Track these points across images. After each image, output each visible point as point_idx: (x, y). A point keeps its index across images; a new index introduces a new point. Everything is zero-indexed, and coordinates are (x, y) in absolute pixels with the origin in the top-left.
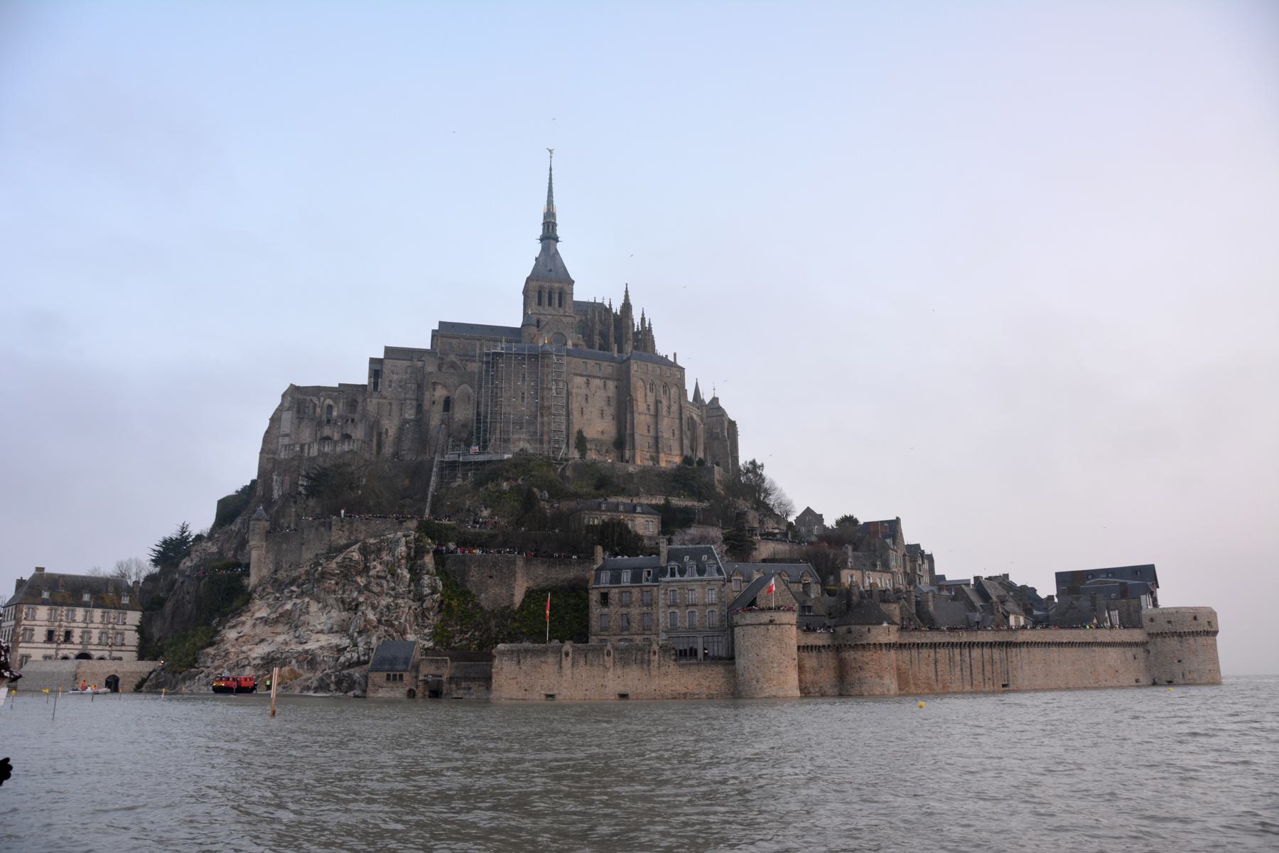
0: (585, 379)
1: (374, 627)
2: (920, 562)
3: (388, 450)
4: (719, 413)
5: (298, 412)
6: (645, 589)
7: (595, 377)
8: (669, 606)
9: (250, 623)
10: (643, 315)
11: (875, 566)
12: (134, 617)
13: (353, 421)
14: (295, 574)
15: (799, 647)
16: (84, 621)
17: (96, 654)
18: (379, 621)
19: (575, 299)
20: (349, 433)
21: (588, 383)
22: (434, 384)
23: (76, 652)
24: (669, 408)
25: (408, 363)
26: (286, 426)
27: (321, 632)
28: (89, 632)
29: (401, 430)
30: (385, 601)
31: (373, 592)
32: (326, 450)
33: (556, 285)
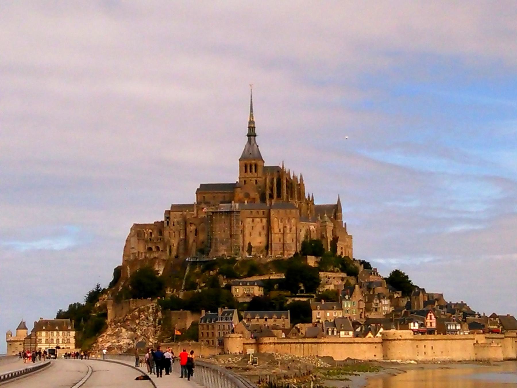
0: (251, 219)
1: (139, 337)
2: (378, 302)
5: (138, 236)
8: (218, 330)
9: (105, 336)
10: (294, 174)
11: (333, 308)
12: (73, 333)
14: (120, 318)
15: (244, 344)
16: (57, 336)
17: (61, 347)
18: (141, 335)
20: (158, 246)
21: (253, 221)
22: (191, 223)
23: (55, 346)
24: (291, 229)
25: (181, 213)
27: (125, 339)
28: (59, 339)
29: (179, 244)
30: (145, 328)
31: (140, 325)
33: (253, 162)
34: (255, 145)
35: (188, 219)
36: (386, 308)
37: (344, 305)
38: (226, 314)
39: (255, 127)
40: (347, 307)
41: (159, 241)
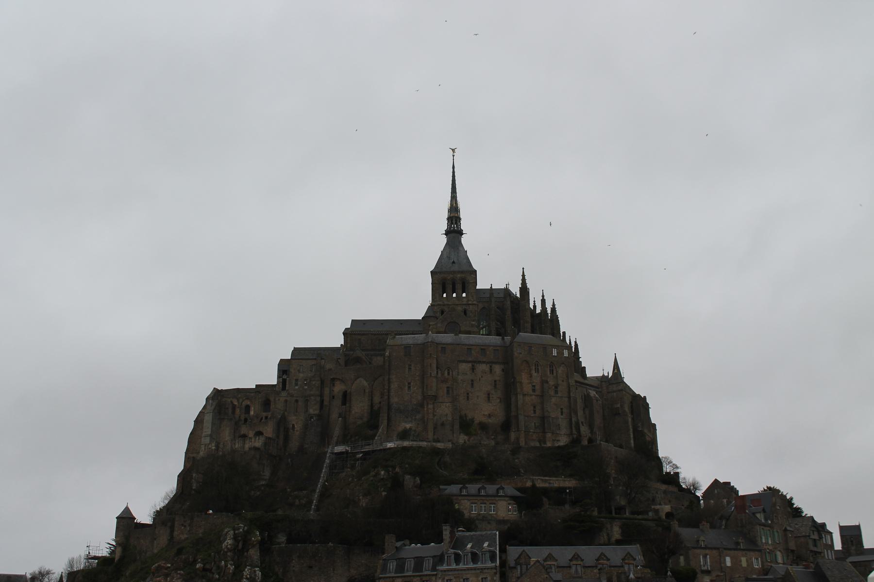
0: (470, 365)
2: (816, 537)
3: (294, 444)
4: (620, 388)
6: (424, 578)
7: (480, 362)
10: (543, 296)
11: (738, 544)
13: (266, 418)
19: (479, 286)
20: (261, 429)
21: (473, 369)
22: (333, 380)
25: (314, 362)
26: (207, 429)
32: (237, 446)
34: (461, 249)
35: (330, 370)
36: (829, 551)
37: (761, 538)
38: (469, 546)
39: (460, 219)
40: (765, 543)
41: (264, 418)
